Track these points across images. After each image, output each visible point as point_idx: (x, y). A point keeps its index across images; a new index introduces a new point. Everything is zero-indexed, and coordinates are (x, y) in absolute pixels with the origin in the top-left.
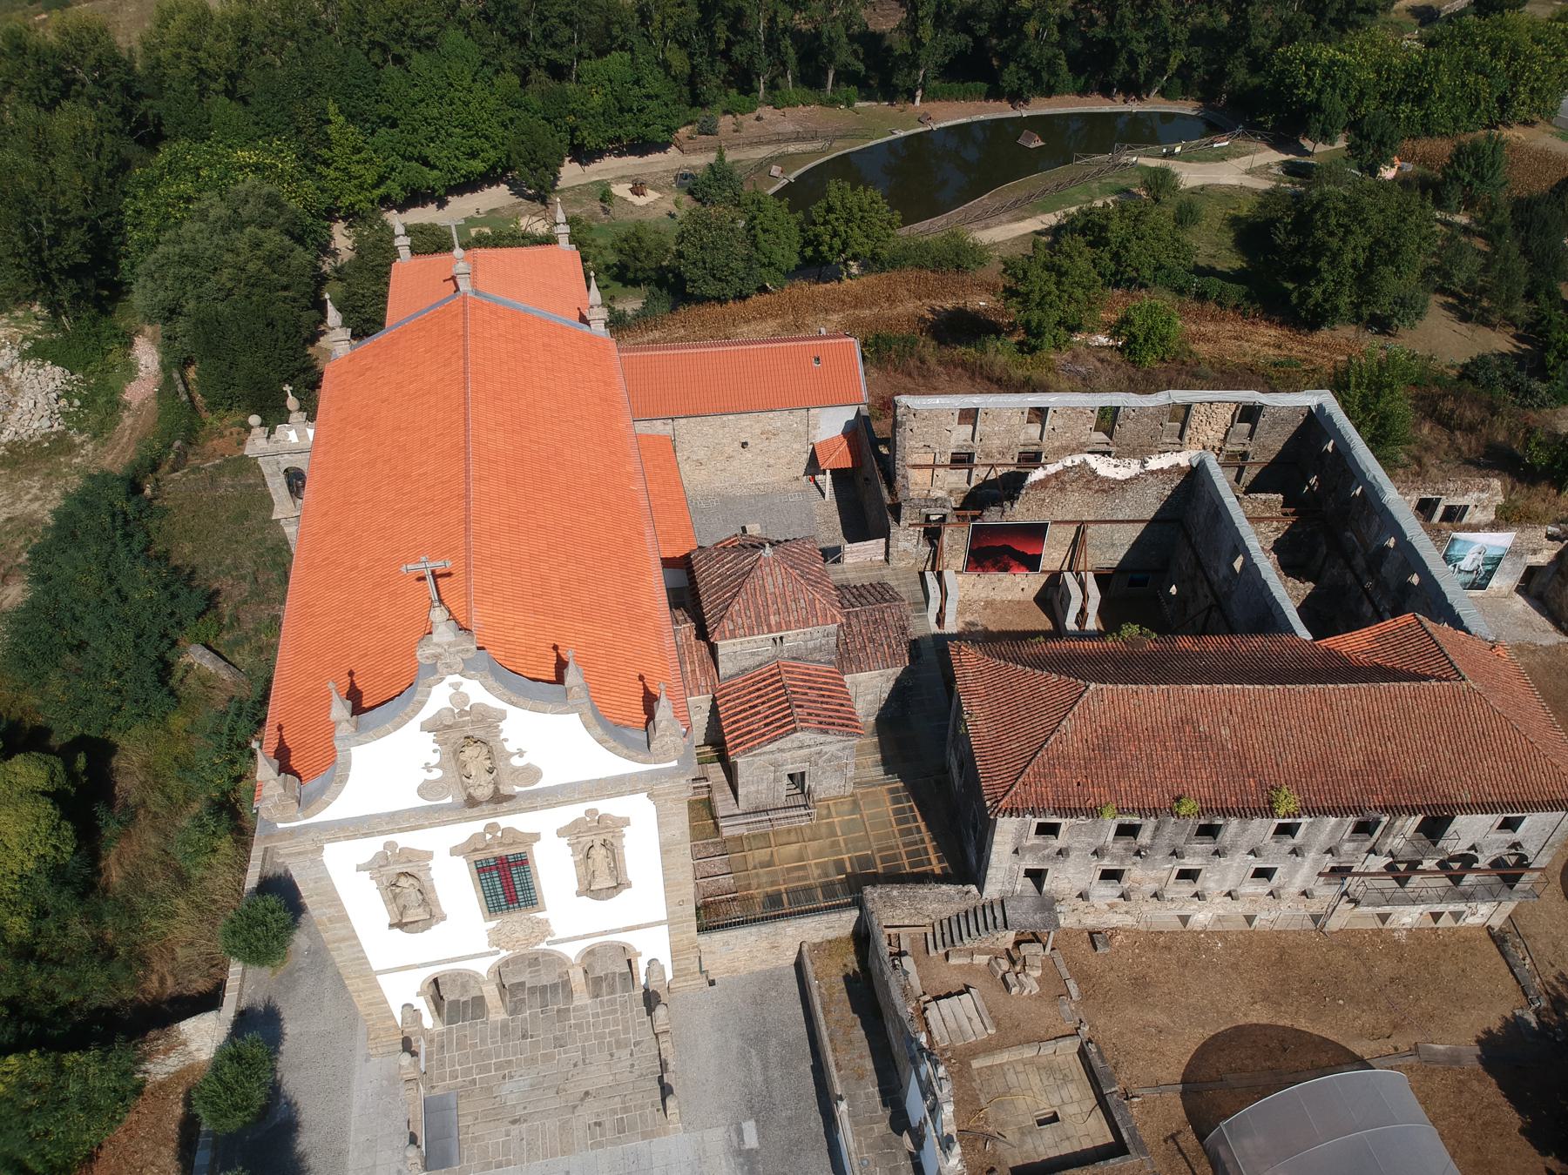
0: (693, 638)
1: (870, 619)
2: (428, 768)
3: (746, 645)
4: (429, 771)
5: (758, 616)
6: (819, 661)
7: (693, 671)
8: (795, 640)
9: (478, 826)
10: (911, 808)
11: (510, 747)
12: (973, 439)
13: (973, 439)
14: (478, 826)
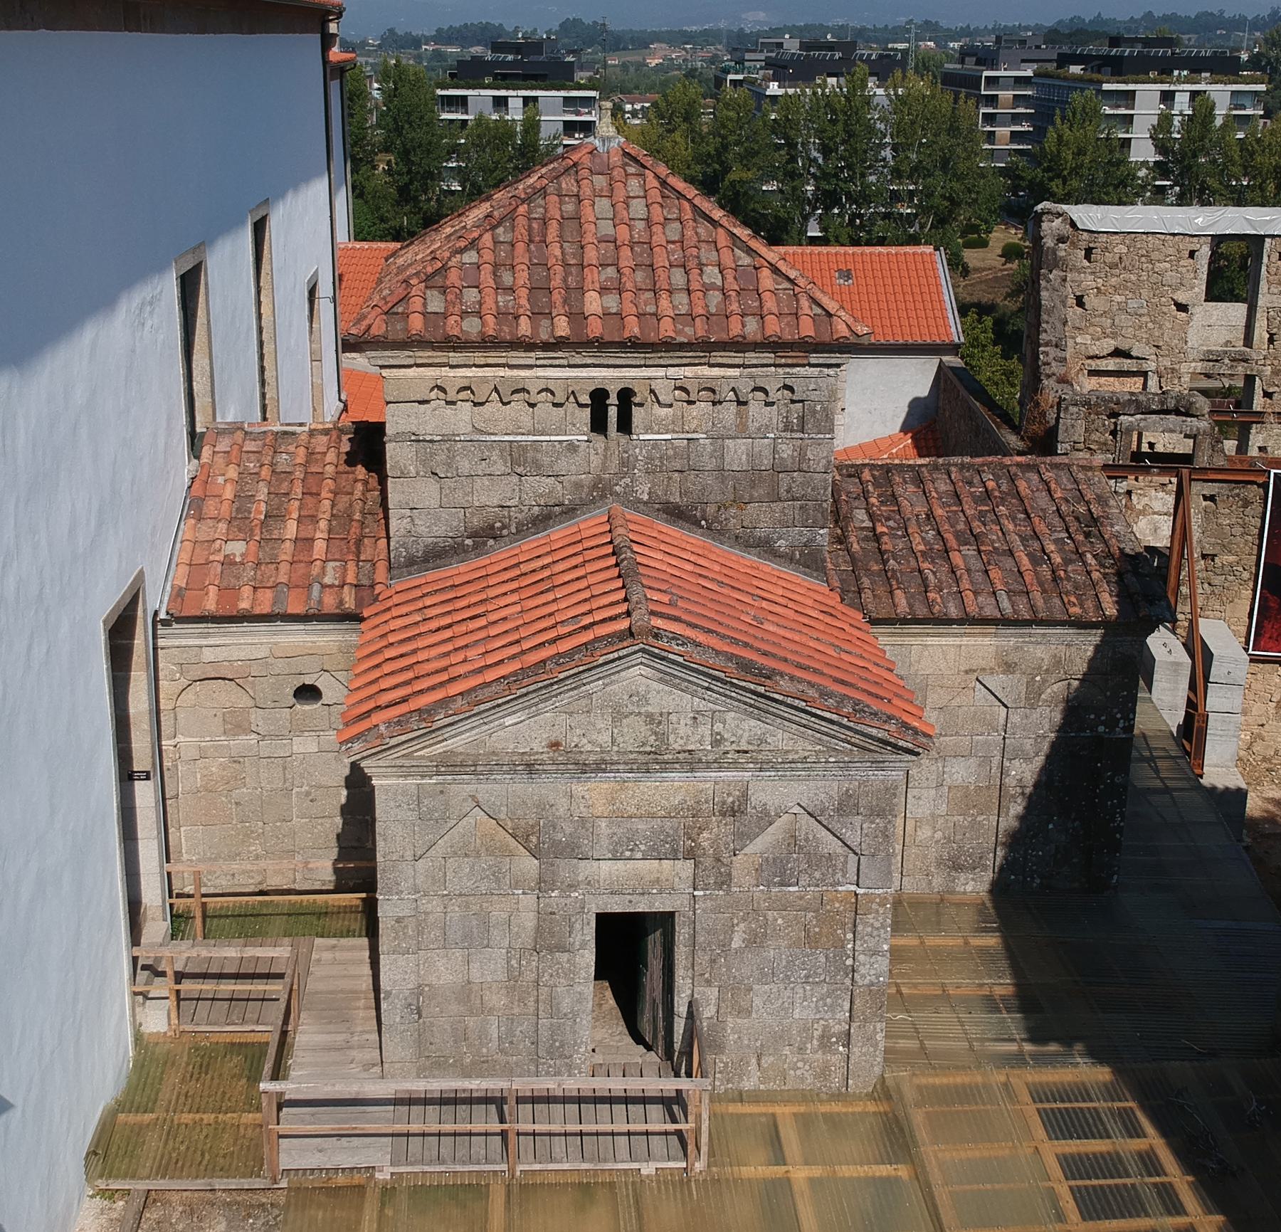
0: (331, 456)
1: (964, 490)
3: (494, 407)
5: (539, 289)
6: (765, 547)
7: (304, 542)
8: (678, 424)
10: (1149, 1163)
12: (1248, 340)
13: (1248, 340)
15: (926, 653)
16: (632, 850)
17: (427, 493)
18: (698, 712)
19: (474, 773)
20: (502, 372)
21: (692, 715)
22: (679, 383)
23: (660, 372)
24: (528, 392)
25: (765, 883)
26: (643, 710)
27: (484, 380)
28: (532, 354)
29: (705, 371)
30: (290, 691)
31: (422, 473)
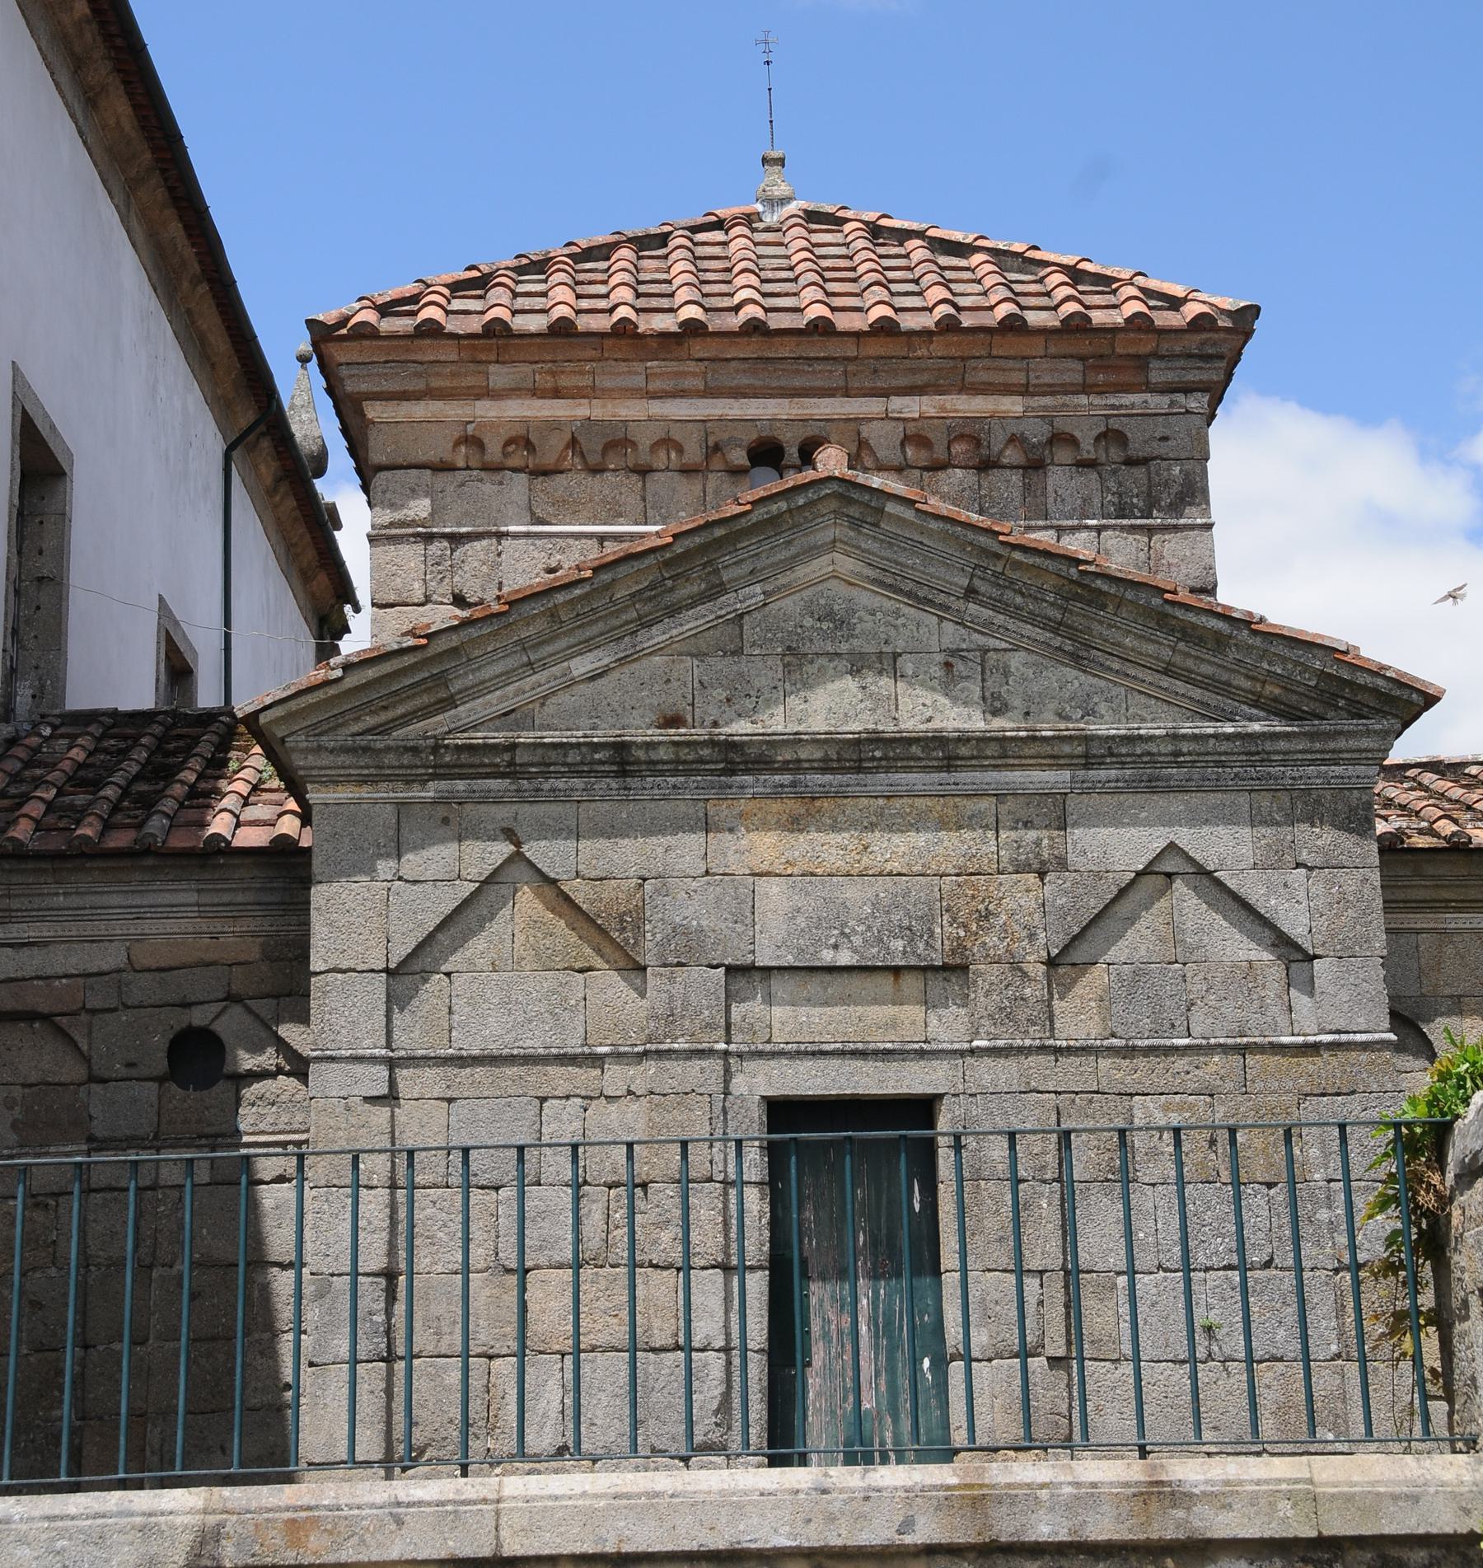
15: (1449, 950)
16: (836, 947)
18: (954, 652)
19: (513, 772)
20: (580, 410)
21: (940, 658)
22: (912, 429)
23: (874, 406)
24: (634, 444)
25: (1119, 1031)
26: (844, 648)
27: (554, 425)
28: (638, 367)
30: (159, 1041)
31: (435, 597)
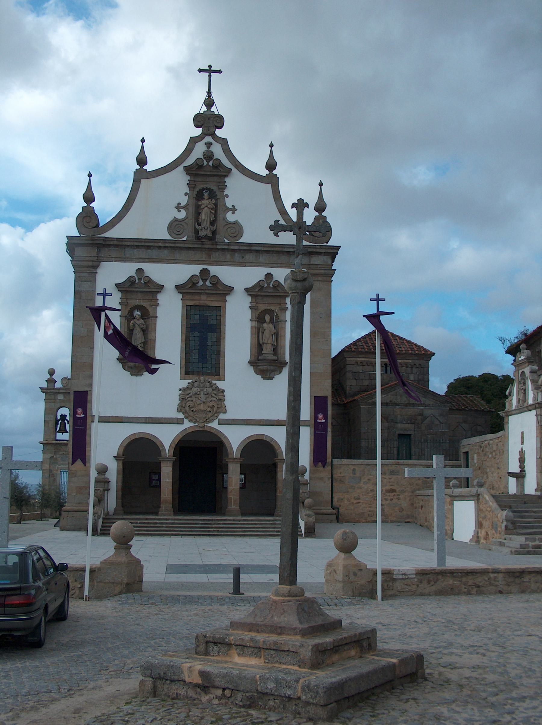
2: (178, 207)
4: (179, 211)
9: (195, 269)
11: (229, 203)
14: (195, 269)
17: (354, 382)
20: (368, 360)
27: (365, 361)
29: (405, 361)
